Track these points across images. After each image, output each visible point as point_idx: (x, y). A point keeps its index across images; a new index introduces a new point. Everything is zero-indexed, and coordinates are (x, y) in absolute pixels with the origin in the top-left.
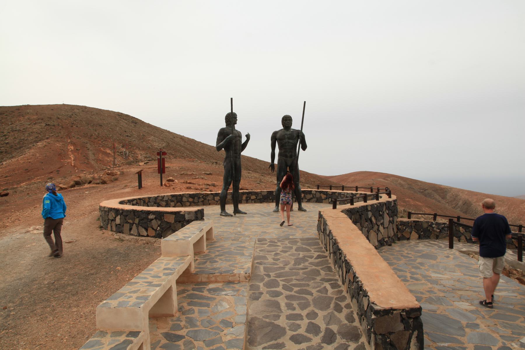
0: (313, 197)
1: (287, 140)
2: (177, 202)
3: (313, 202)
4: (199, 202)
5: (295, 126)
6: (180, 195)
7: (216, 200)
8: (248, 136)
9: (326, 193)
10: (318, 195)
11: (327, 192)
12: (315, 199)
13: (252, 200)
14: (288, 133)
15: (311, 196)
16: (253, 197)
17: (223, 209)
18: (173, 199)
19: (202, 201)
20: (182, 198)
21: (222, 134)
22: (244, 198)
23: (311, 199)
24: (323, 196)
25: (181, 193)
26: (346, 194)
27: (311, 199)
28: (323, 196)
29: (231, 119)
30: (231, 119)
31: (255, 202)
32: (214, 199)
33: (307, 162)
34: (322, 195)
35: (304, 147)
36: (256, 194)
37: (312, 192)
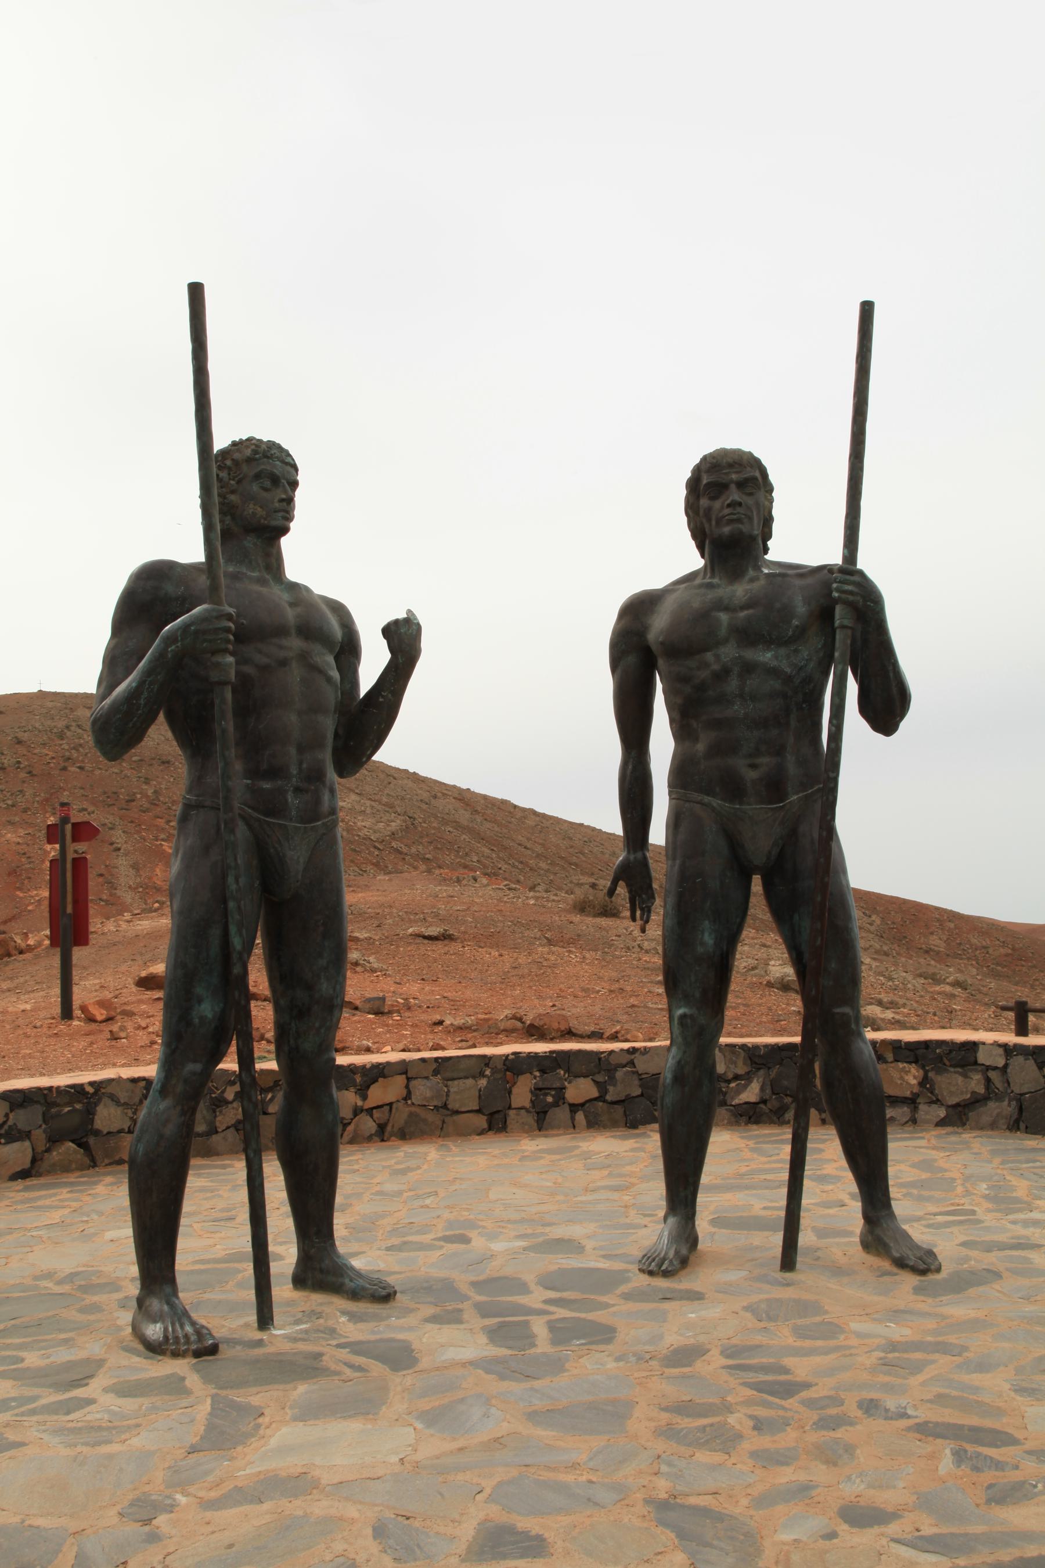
0: (990, 1094)
2: (54, 1140)
3: (993, 1126)
4: (213, 1131)
6: (78, 1090)
12: (1006, 1108)
13: (574, 1108)
15: (975, 1083)
16: (580, 1089)
18: (20, 1119)
20: (90, 1113)
22: (522, 1093)
23: (976, 1101)
25: (83, 1078)
27: (976, 1101)
31: (594, 1124)
36: (598, 1066)
37: (982, 1057)
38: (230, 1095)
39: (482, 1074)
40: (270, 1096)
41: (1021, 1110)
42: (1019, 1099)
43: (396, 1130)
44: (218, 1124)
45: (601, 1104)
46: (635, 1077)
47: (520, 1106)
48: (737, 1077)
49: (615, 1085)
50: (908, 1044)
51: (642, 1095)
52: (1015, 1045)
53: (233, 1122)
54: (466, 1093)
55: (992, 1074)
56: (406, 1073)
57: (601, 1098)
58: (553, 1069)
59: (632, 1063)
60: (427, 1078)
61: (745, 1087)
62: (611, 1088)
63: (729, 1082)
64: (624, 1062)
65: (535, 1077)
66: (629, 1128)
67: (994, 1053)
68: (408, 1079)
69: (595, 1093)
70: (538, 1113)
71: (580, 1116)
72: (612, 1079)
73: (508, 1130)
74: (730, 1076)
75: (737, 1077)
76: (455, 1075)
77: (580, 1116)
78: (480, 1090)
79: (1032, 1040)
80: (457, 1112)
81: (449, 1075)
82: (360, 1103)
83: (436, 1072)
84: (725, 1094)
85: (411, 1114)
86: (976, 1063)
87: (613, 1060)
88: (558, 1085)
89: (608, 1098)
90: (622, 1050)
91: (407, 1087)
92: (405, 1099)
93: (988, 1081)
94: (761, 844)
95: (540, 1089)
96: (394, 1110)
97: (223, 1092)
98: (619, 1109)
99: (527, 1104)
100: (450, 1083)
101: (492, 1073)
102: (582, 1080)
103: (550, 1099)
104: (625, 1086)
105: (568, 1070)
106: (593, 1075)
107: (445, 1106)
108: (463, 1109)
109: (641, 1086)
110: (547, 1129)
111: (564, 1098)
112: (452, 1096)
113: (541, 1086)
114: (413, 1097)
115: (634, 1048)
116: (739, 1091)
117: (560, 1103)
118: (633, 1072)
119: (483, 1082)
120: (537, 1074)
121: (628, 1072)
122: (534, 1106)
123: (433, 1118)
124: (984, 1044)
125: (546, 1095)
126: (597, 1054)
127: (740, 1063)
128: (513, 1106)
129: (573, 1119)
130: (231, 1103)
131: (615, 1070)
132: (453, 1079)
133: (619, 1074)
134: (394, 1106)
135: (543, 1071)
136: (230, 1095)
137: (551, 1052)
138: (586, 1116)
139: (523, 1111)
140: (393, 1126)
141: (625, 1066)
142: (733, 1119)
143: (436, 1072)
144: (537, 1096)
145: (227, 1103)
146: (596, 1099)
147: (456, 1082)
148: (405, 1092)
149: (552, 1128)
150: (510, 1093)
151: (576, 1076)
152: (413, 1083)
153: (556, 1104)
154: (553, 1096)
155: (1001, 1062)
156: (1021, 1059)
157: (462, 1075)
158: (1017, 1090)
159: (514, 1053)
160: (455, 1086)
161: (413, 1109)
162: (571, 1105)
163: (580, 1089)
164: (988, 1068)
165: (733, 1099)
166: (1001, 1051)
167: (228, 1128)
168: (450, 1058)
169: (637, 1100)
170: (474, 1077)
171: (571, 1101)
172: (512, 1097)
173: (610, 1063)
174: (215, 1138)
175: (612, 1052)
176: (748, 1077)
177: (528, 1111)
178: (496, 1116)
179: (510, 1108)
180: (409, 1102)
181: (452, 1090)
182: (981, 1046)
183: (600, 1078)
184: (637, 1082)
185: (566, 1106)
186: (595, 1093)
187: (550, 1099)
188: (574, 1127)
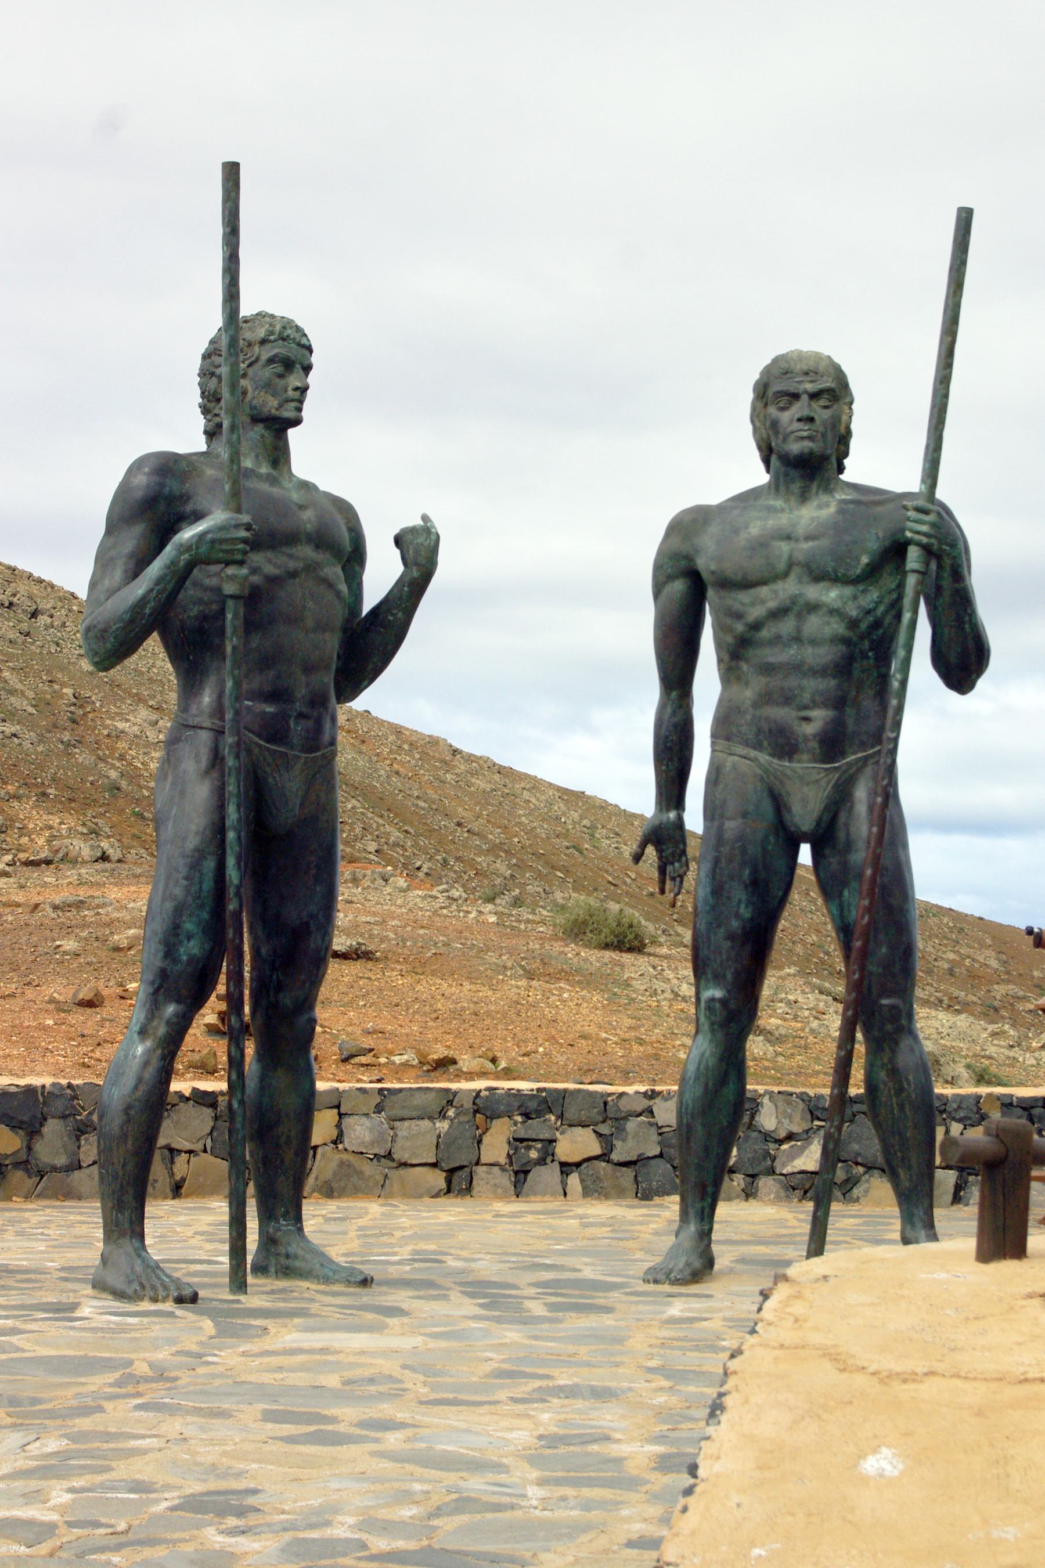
1: (788, 588)
5: (880, 459)
8: (420, 551)
13: (566, 1168)
14: (816, 512)
16: (576, 1143)
17: (126, 1220)
21: (154, 503)
22: (496, 1145)
29: (258, 378)
30: (258, 378)
35: (963, 661)
39: (442, 1114)
43: (319, 1183)
44: (82, 1157)
45: (604, 1164)
46: (654, 1130)
47: (492, 1161)
48: (790, 1137)
49: (624, 1140)
50: (1021, 1100)
51: (661, 1155)
54: (419, 1138)
56: (338, 1107)
57: (604, 1157)
58: (539, 1113)
59: (650, 1112)
60: (367, 1115)
61: (803, 1149)
62: (618, 1144)
63: (780, 1142)
64: (639, 1109)
66: (642, 1199)
68: (340, 1115)
69: (595, 1148)
70: (516, 1173)
71: (574, 1180)
72: (621, 1130)
73: (474, 1193)
74: (782, 1134)
75: (790, 1137)
76: (406, 1113)
78: (439, 1136)
80: (405, 1165)
81: (399, 1113)
83: (379, 1109)
84: (774, 1159)
85: (342, 1163)
87: (624, 1105)
88: (547, 1136)
89: (615, 1157)
90: (637, 1093)
91: (339, 1126)
92: (335, 1142)
94: (806, 806)
95: (522, 1140)
96: (318, 1156)
98: (629, 1173)
99: (503, 1160)
100: (397, 1124)
101: (457, 1115)
102: (579, 1130)
105: (561, 1117)
106: (596, 1124)
107: (389, 1155)
108: (414, 1162)
109: (659, 1143)
110: (527, 1195)
112: (400, 1142)
113: (522, 1134)
114: (346, 1140)
116: (792, 1156)
117: (549, 1160)
118: (651, 1124)
119: (443, 1126)
120: (519, 1119)
121: (644, 1122)
122: (511, 1164)
123: (369, 1169)
125: (528, 1148)
127: (797, 1117)
128: (483, 1160)
129: (564, 1185)
131: (626, 1118)
132: (402, 1119)
133: (631, 1125)
134: (320, 1151)
135: (527, 1116)
138: (582, 1181)
139: (496, 1168)
140: (317, 1178)
141: (640, 1115)
142: (783, 1193)
143: (379, 1109)
144: (516, 1149)
147: (406, 1123)
148: (335, 1133)
149: (535, 1194)
150: (480, 1142)
151: (570, 1126)
152: (347, 1121)
153: (541, 1161)
154: (538, 1151)
157: (414, 1114)
159: (488, 1089)
160: (404, 1129)
161: (345, 1156)
162: (563, 1164)
165: (784, 1165)
167: (95, 1163)
169: (653, 1162)
170: (431, 1118)
171: (563, 1159)
172: (482, 1147)
173: (619, 1110)
175: (622, 1095)
176: (806, 1136)
178: (460, 1173)
179: (477, 1163)
180: (340, 1146)
181: (399, 1133)
183: (604, 1129)
184: (655, 1138)
185: (556, 1165)
186: (595, 1148)
188: (565, 1194)
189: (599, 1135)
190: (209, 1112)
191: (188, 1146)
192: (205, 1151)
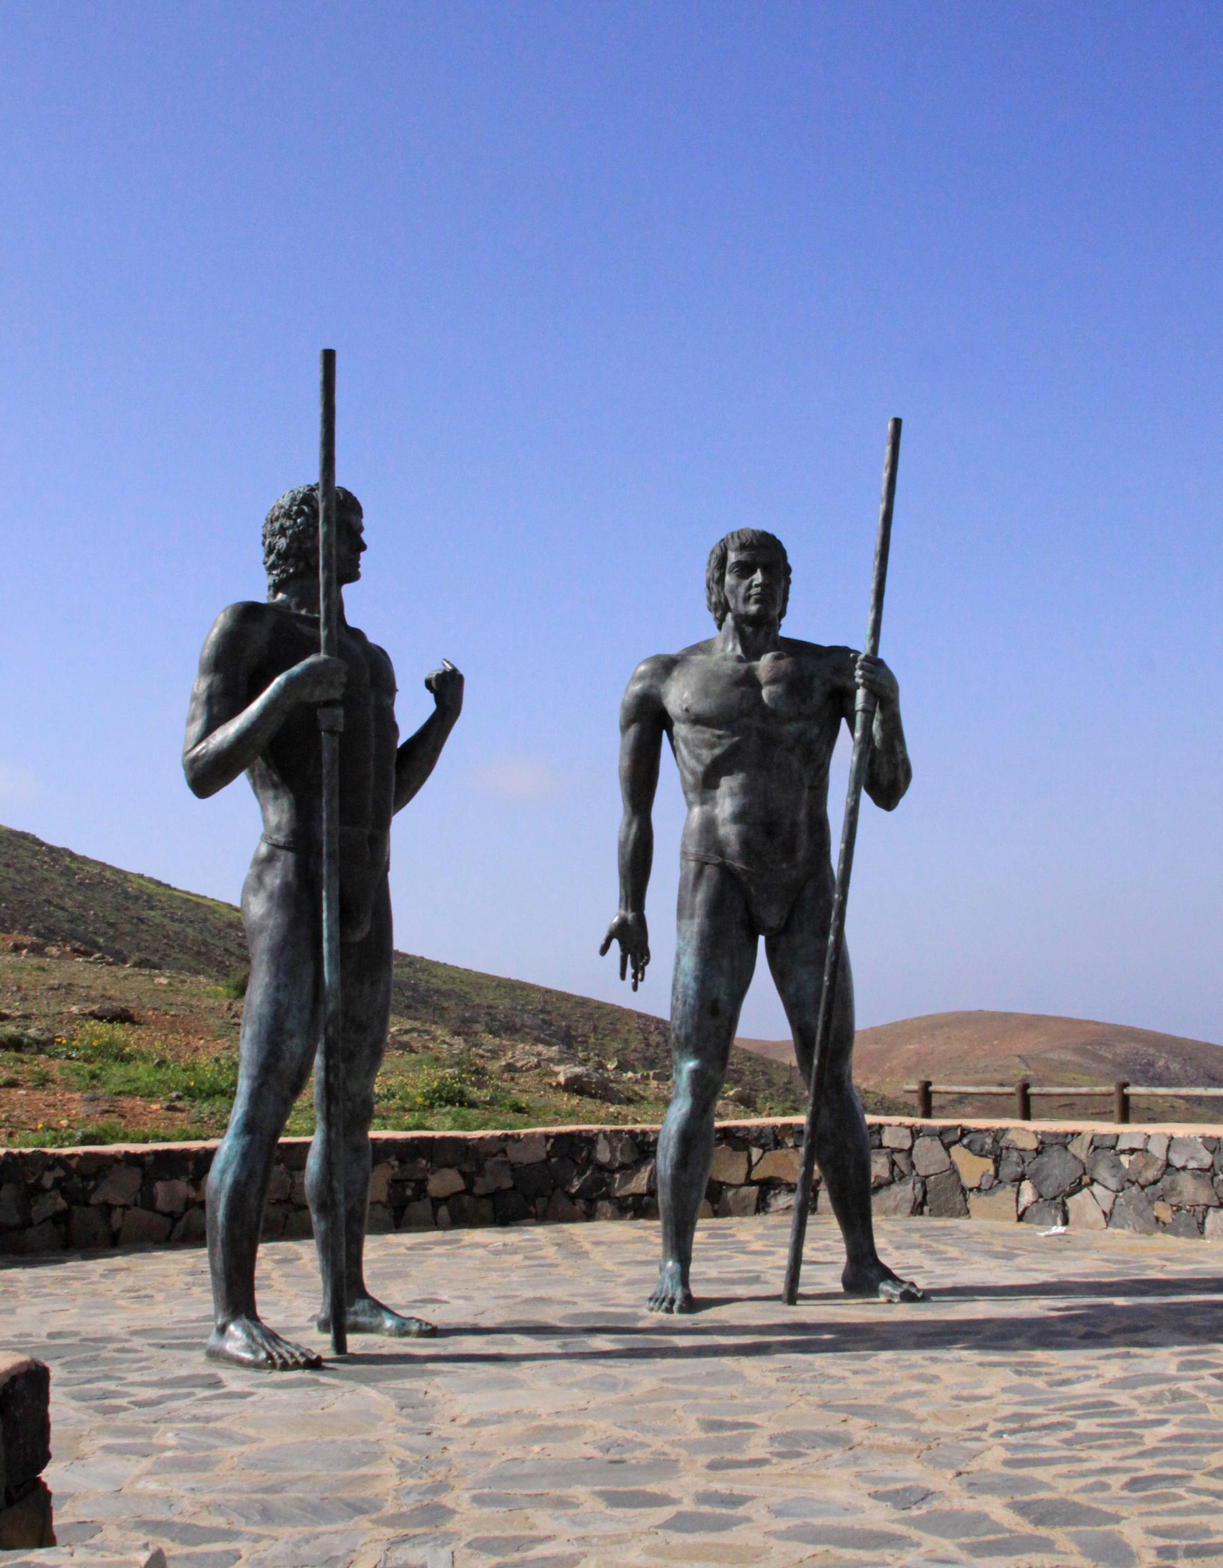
4: (27, 1223)
7: (161, 1204)
9: (996, 1149)
10: (929, 1157)
11: (1005, 1131)
13: (437, 1202)
16: (445, 1182)
19: (61, 1218)
24: (973, 1168)
26: (1157, 1150)
28: (973, 1168)
32: (148, 1202)
33: (933, 916)
34: (958, 1152)
35: (885, 778)
38: (48, 1180)
40: (92, 1184)
41: (925, 1193)
42: (924, 1181)
44: (33, 1215)
45: (467, 1197)
48: (623, 1167)
49: (483, 1176)
51: (514, 1188)
52: (922, 1126)
53: (50, 1214)
55: (898, 1157)
57: (468, 1191)
59: (504, 1151)
62: (479, 1180)
64: (494, 1151)
65: (393, 1167)
67: (901, 1135)
71: (443, 1211)
72: (480, 1170)
77: (443, 1211)
79: (937, 1122)
82: (193, 1194)
86: (881, 1146)
88: (420, 1176)
89: (477, 1190)
90: (492, 1137)
93: (893, 1164)
97: (40, 1178)
102: (446, 1171)
103: (409, 1192)
104: (496, 1179)
105: (430, 1159)
107: (288, 1200)
109: (513, 1178)
111: (425, 1191)
115: (506, 1135)
118: (505, 1162)
124: (890, 1125)
126: (465, 1140)
129: (435, 1214)
130: (49, 1191)
133: (489, 1164)
135: (402, 1162)
136: (48, 1180)
137: (413, 1139)
141: (495, 1155)
145: (44, 1191)
146: (462, 1192)
155: (907, 1144)
156: (928, 1139)
158: (922, 1173)
163: (445, 1182)
164: (894, 1150)
166: (908, 1132)
167: (45, 1220)
168: (297, 1144)
171: (434, 1194)
174: (30, 1233)
177: (384, 1206)
182: (887, 1128)
183: (467, 1168)
184: (509, 1173)
185: (427, 1202)
187: (409, 1192)
189: (463, 1174)
190: (137, 1172)
191: (122, 1201)
192: (136, 1205)
